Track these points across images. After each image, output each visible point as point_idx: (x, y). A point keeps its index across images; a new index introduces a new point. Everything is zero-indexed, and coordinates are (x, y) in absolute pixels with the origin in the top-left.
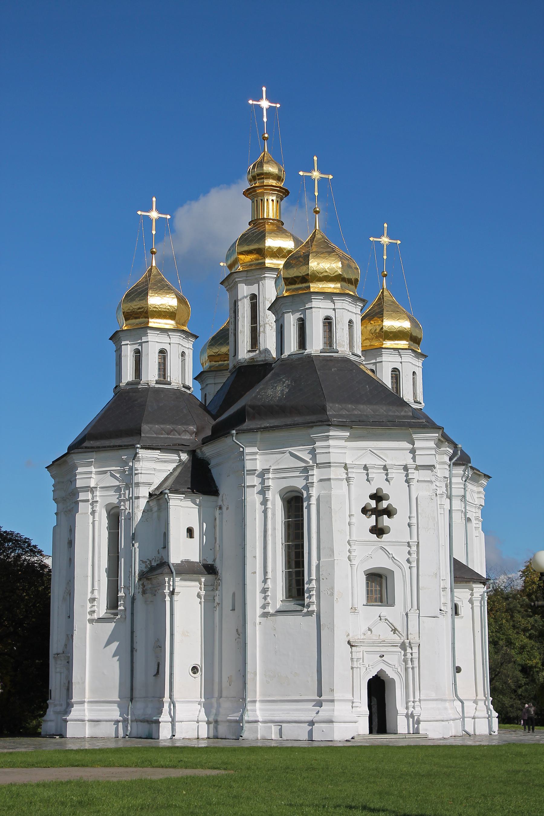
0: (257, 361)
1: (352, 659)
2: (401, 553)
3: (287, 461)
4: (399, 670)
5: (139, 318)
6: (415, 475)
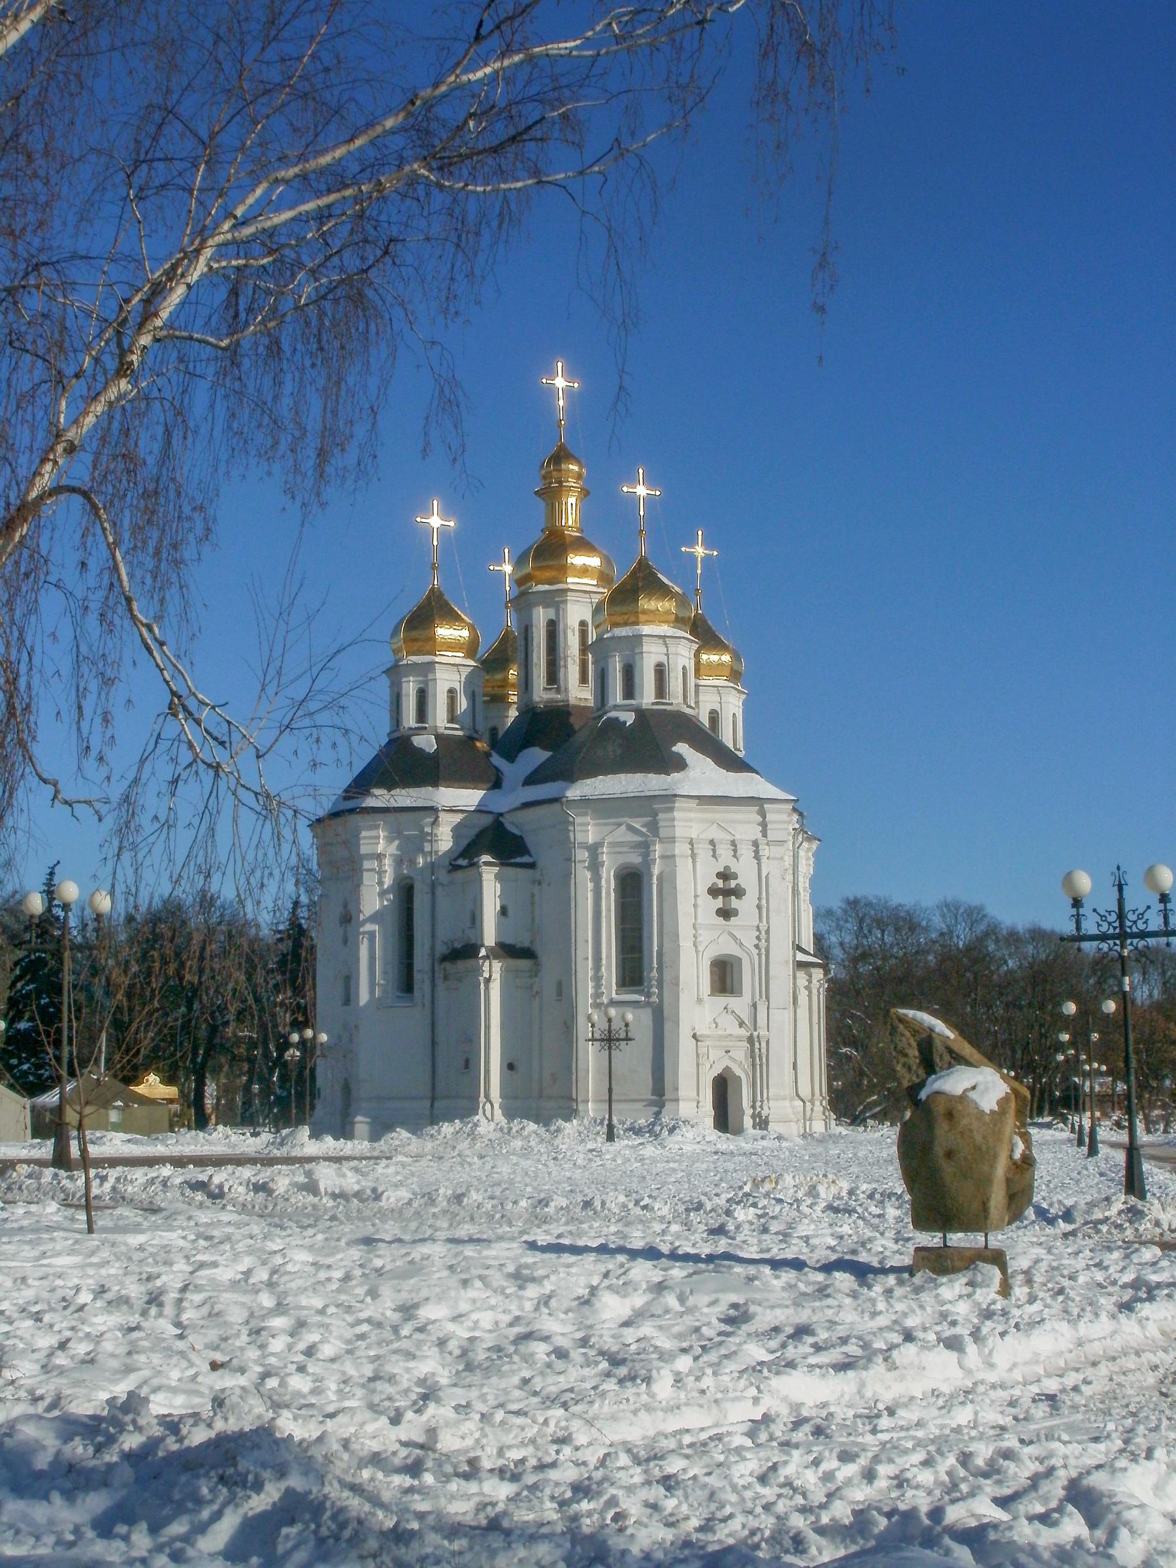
2: (749, 940)
6: (765, 851)
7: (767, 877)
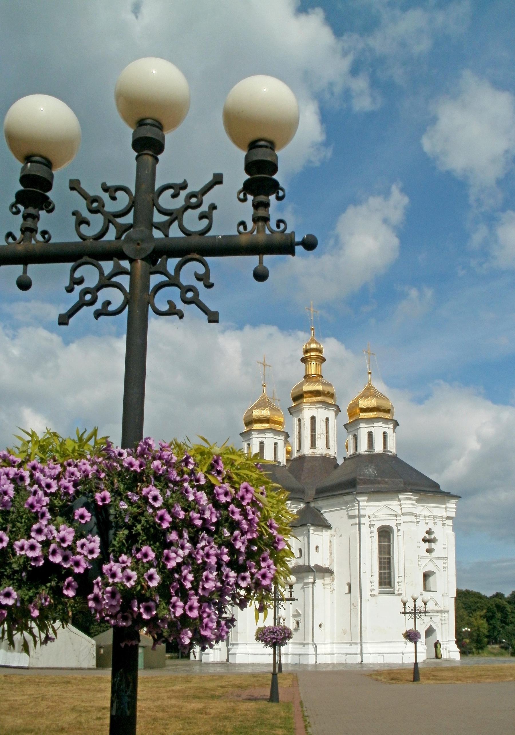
0: (316, 454)
3: (385, 511)
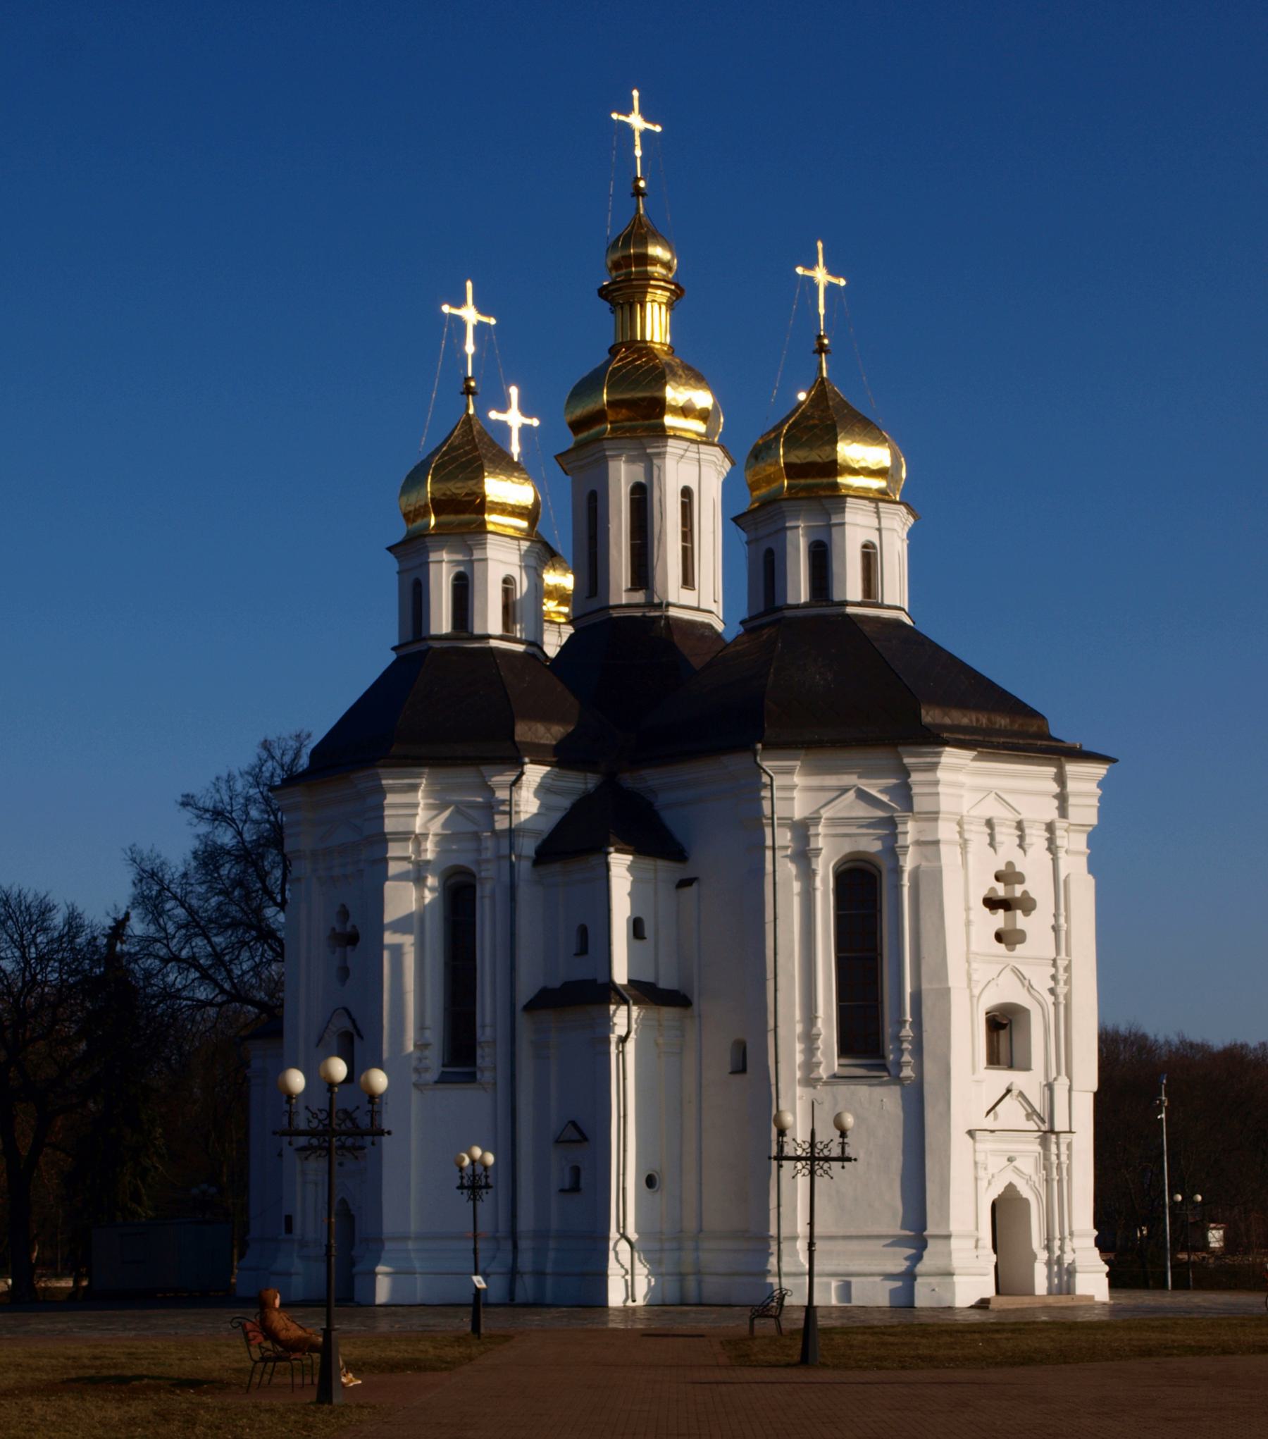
1: (976, 1163)
4: (1037, 1185)
5: (463, 512)
6: (1062, 840)
7: (1066, 881)
